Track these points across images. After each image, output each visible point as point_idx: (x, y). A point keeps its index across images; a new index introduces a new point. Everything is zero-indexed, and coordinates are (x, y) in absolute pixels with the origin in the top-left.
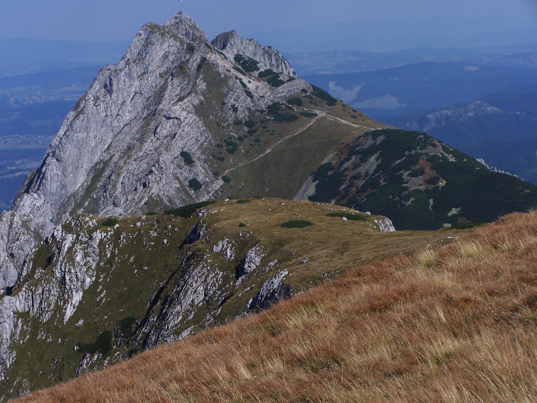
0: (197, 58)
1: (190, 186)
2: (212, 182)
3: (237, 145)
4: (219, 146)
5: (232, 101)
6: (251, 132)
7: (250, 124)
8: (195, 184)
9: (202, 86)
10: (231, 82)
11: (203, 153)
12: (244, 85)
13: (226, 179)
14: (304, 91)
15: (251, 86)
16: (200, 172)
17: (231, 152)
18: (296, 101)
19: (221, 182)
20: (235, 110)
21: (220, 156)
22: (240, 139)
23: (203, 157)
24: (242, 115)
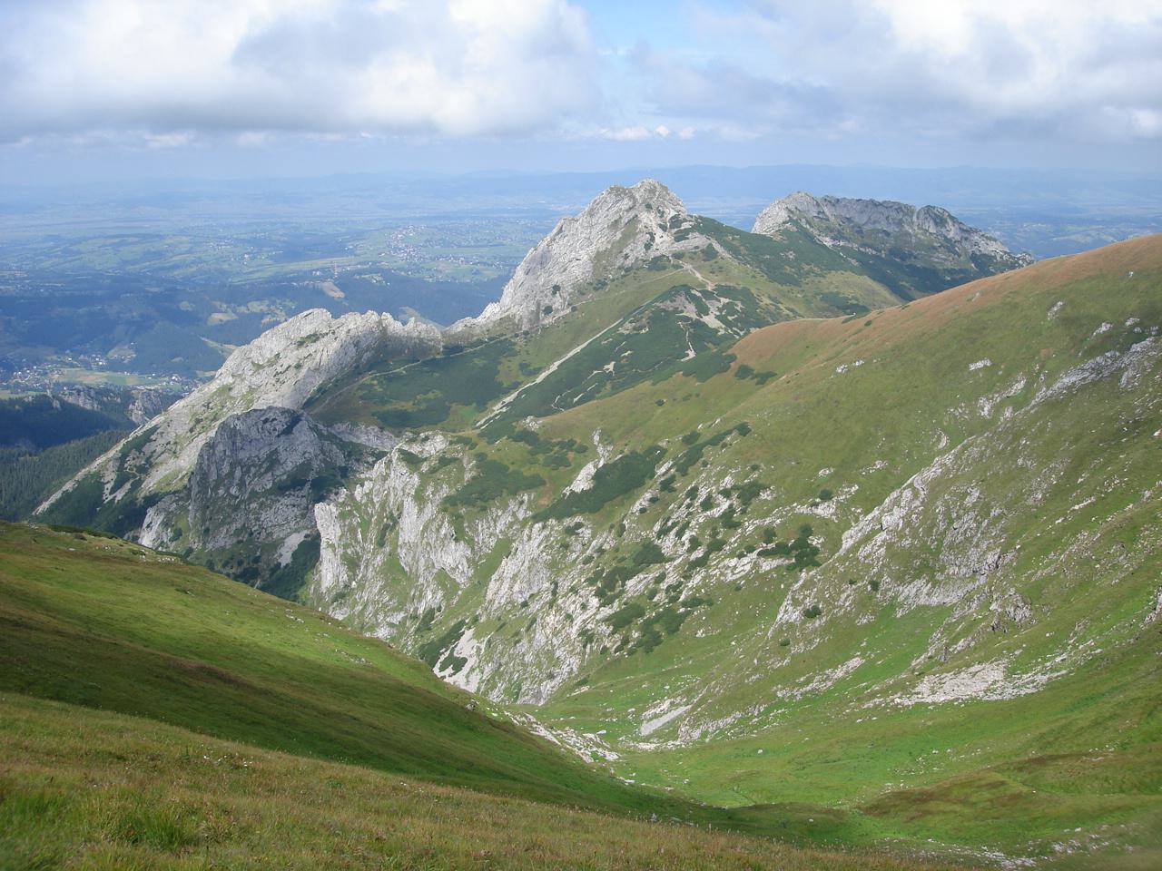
0: (631, 214)
1: (544, 311)
2: (563, 310)
3: (607, 284)
4: (591, 284)
5: (628, 251)
6: (624, 276)
7: (628, 270)
8: (548, 310)
9: (619, 235)
10: (639, 236)
11: (573, 288)
12: (653, 239)
13: (574, 309)
14: (697, 247)
15: (658, 240)
16: (557, 302)
17: (596, 289)
18: (678, 256)
19: (568, 311)
20: (626, 257)
21: (585, 291)
22: (613, 280)
23: (571, 291)
24: (629, 262)
